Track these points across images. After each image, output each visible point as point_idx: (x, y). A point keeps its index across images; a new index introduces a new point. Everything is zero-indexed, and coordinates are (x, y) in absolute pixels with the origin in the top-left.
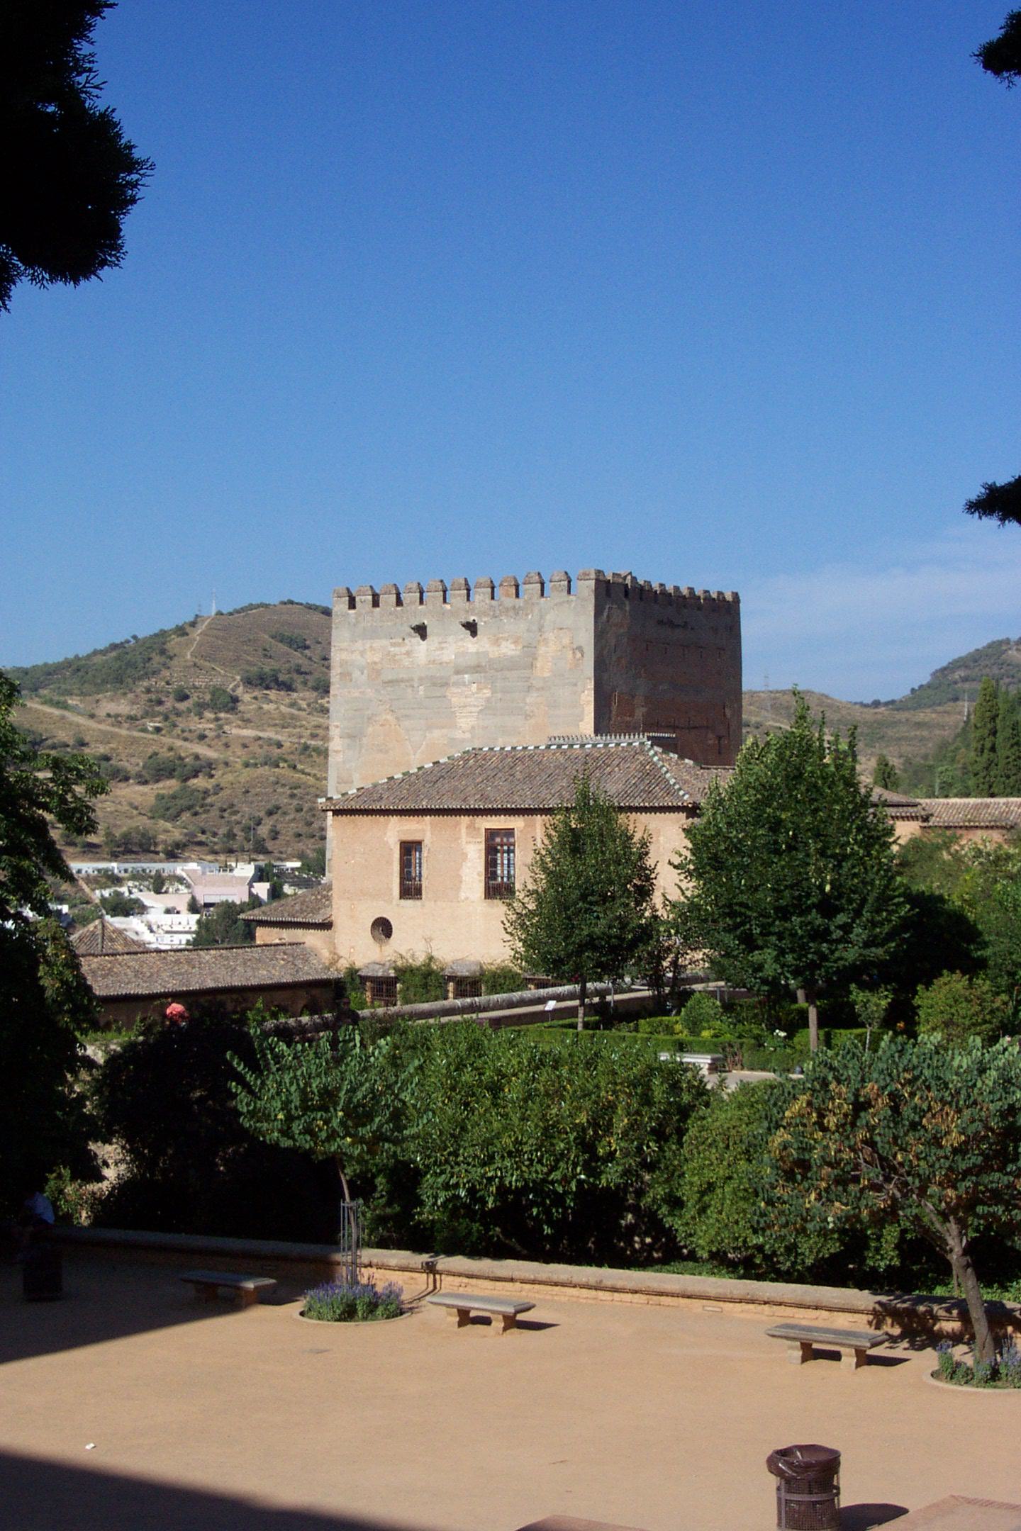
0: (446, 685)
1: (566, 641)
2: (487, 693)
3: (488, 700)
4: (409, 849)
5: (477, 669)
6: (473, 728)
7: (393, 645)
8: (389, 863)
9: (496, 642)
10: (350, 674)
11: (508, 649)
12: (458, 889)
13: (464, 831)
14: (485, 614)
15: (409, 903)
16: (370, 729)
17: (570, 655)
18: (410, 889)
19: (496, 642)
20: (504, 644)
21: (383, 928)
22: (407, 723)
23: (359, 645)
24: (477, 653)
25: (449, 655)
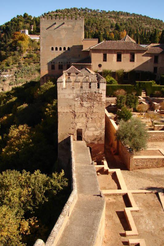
0: (60, 31)
1: (79, 26)
2: (67, 32)
11: (70, 26)
12: (112, 60)
15: (105, 62)
18: (105, 59)
19: (68, 25)
21: (100, 66)
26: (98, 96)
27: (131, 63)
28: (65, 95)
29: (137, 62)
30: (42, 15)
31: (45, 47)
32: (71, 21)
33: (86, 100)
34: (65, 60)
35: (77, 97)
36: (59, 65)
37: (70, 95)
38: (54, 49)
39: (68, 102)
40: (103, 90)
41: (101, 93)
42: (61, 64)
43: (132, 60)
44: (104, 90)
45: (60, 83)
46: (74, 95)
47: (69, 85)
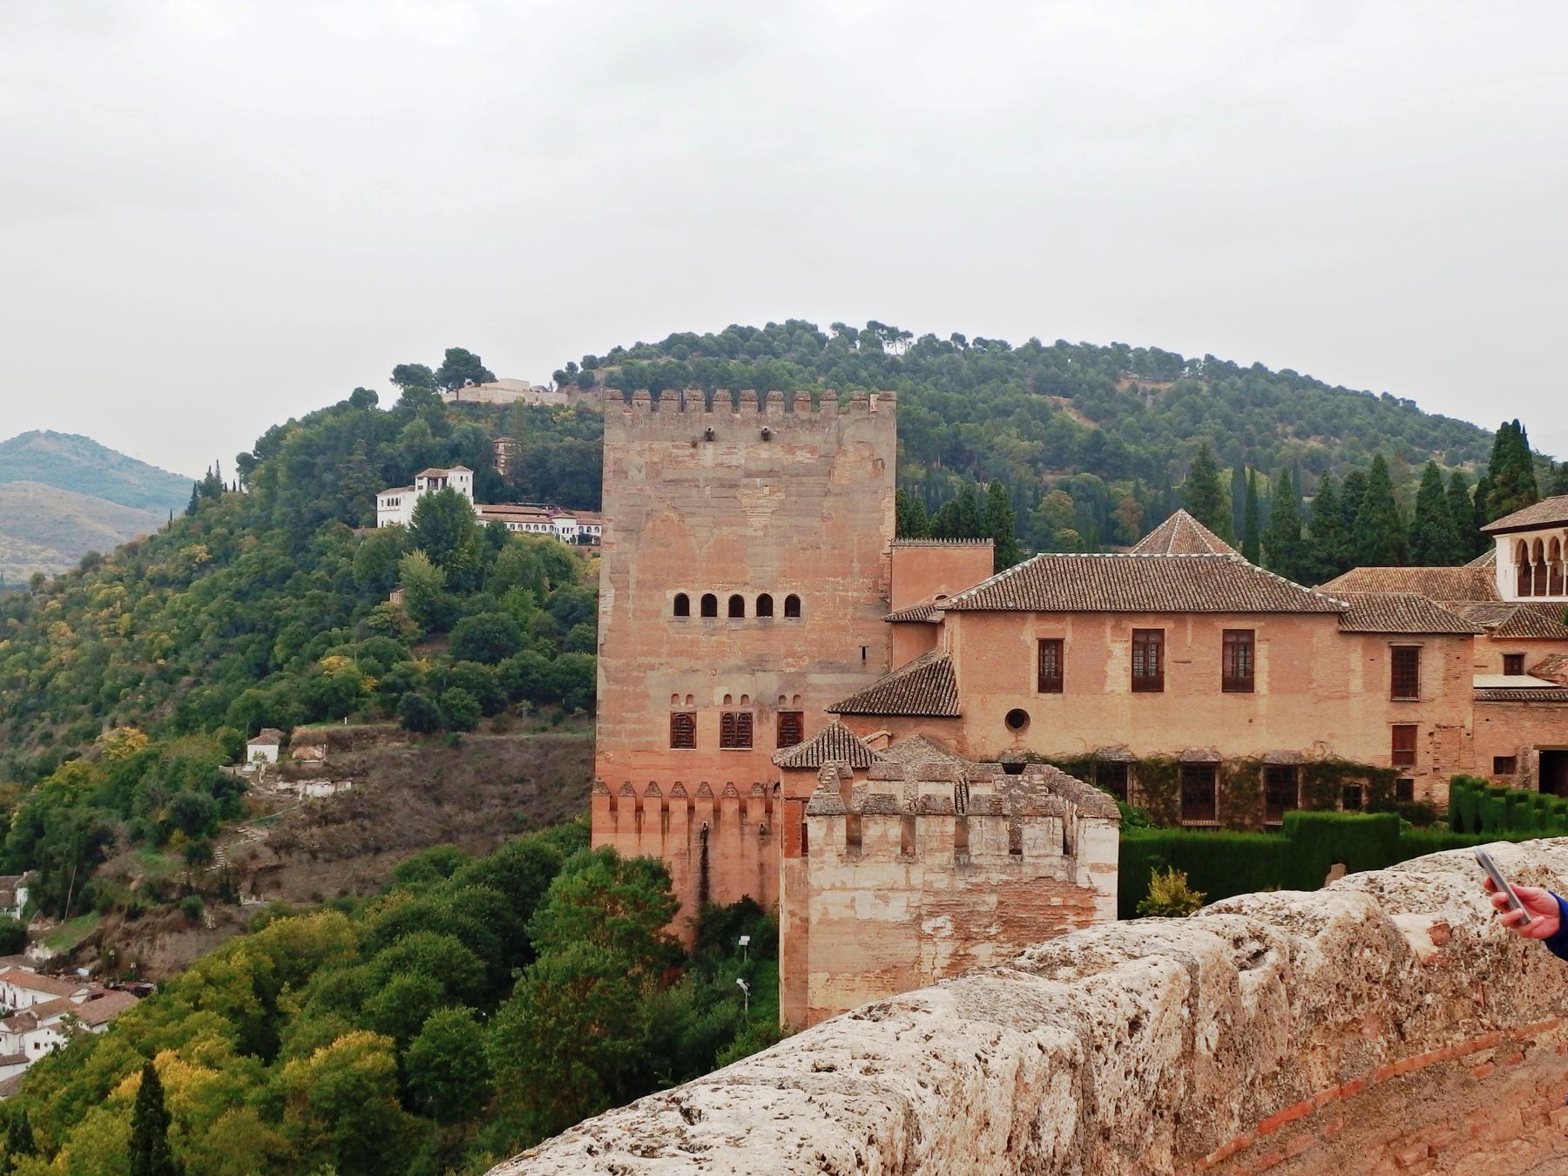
0: (735, 486)
1: (866, 453)
3: (782, 502)
4: (1050, 648)
5: (770, 473)
6: (765, 526)
7: (676, 447)
8: (1027, 659)
9: (791, 450)
10: (626, 473)
11: (803, 457)
13: (1108, 630)
14: (778, 424)
15: (1049, 696)
16: (650, 524)
17: (870, 466)
19: (791, 450)
20: (799, 453)
21: (1017, 720)
22: (691, 520)
23: (637, 446)
24: (770, 459)
25: (739, 458)
26: (1072, 902)
27: (1232, 699)
28: (853, 900)
29: (1271, 690)
30: (571, 366)
31: (631, 592)
32: (812, 423)
33: (993, 931)
34: (769, 684)
35: (931, 914)
36: (727, 719)
37: (886, 901)
38: (695, 606)
39: (874, 943)
40: (1095, 867)
41: (1086, 886)
42: (736, 708)
43: (1238, 682)
44: (1109, 868)
45: (824, 821)
46: (916, 898)
47: (884, 836)
